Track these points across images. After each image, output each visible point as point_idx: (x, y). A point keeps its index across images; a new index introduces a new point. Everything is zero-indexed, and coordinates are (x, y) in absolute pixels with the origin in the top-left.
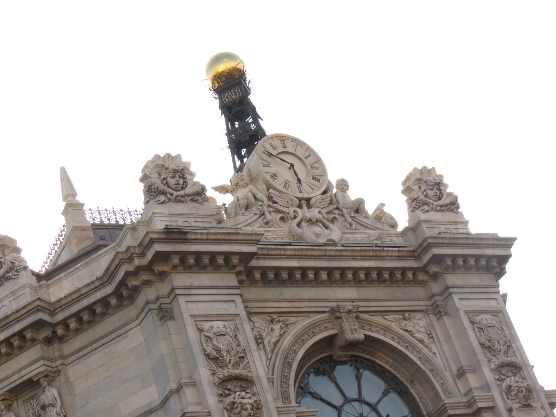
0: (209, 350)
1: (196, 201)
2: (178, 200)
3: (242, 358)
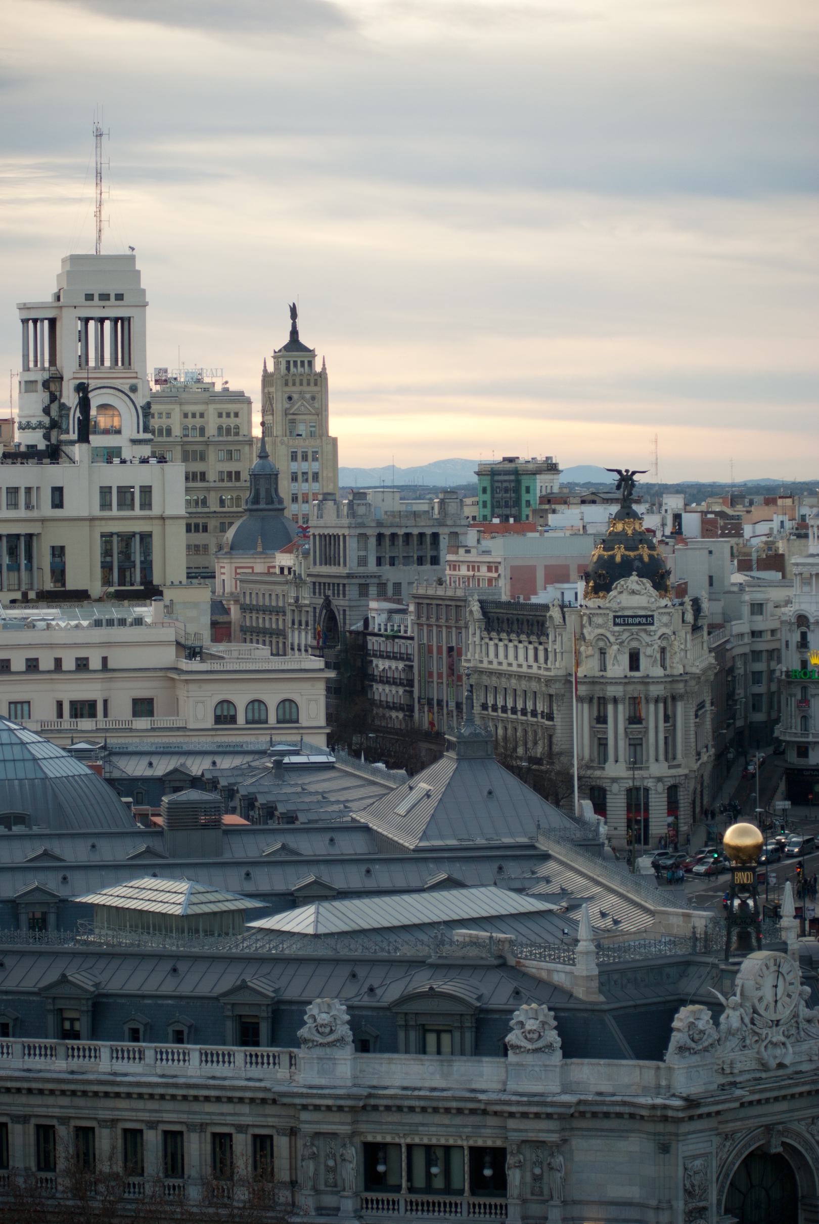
0: (688, 1186)
1: (708, 1051)
2: (695, 1053)
3: (705, 1190)
